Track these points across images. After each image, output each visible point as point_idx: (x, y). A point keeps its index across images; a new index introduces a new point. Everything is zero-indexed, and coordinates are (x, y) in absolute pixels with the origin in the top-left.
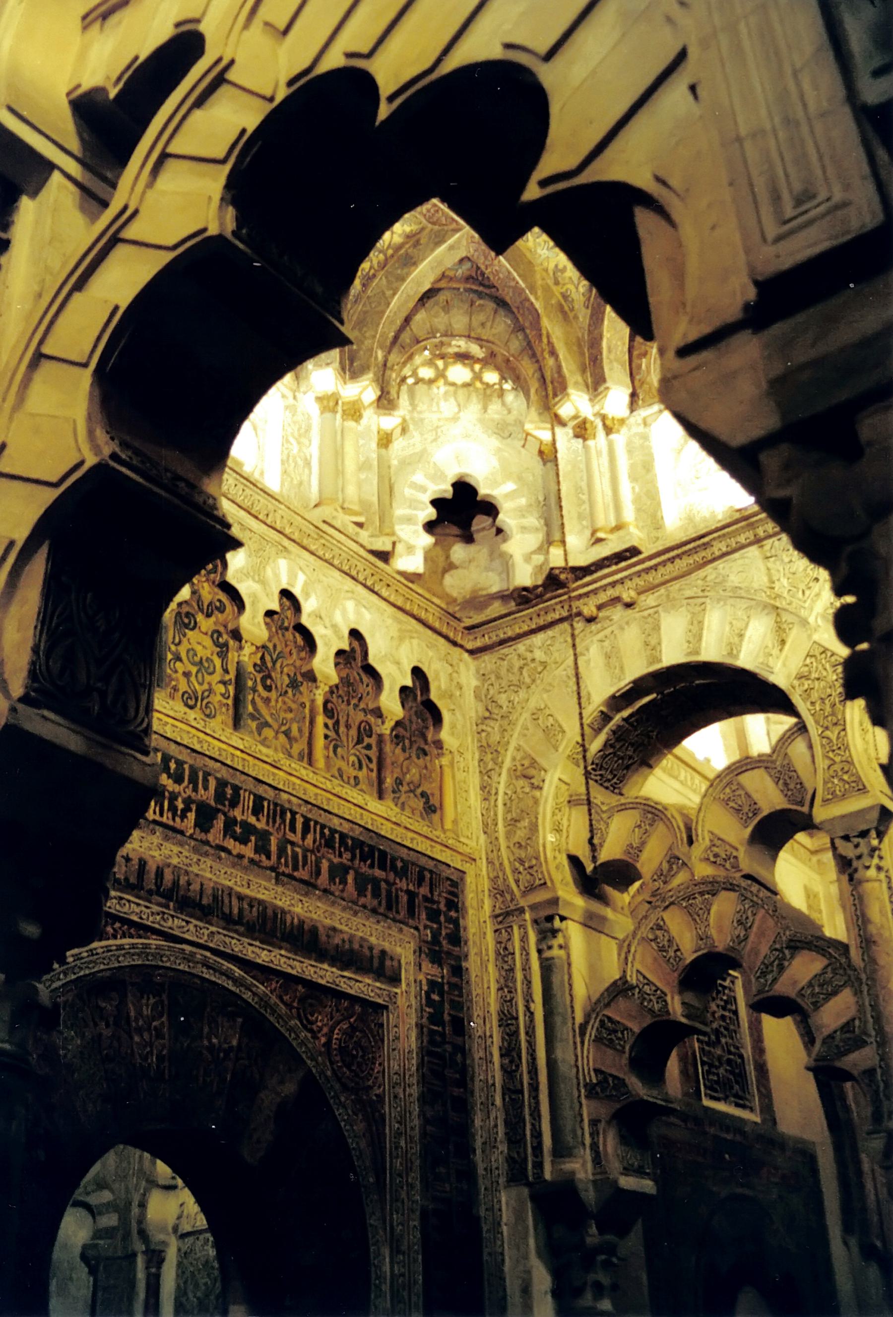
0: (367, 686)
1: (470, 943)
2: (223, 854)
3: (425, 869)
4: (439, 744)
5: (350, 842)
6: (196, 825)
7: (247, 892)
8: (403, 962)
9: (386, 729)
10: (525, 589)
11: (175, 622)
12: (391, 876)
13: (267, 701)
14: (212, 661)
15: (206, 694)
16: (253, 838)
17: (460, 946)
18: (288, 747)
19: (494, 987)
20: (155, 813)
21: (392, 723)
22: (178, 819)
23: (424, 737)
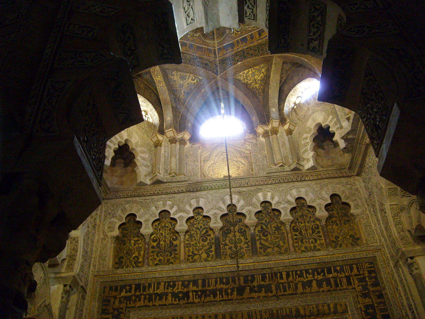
0: (313, 212)
1: (385, 283)
2: (251, 300)
3: (352, 264)
4: (352, 215)
5: (310, 271)
6: (237, 295)
7: (264, 308)
8: (347, 304)
9: (323, 222)
10: (345, 148)
11: (223, 234)
12: (335, 274)
13: (267, 240)
14: (240, 239)
15: (239, 250)
16: (263, 289)
17: (380, 286)
18: (279, 250)
19: (402, 294)
20: (220, 298)
21: (325, 220)
22: (229, 296)
23: (346, 215)
